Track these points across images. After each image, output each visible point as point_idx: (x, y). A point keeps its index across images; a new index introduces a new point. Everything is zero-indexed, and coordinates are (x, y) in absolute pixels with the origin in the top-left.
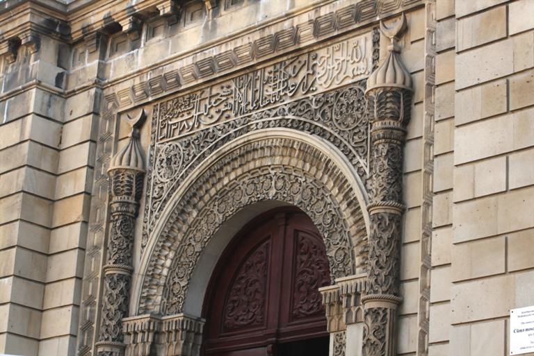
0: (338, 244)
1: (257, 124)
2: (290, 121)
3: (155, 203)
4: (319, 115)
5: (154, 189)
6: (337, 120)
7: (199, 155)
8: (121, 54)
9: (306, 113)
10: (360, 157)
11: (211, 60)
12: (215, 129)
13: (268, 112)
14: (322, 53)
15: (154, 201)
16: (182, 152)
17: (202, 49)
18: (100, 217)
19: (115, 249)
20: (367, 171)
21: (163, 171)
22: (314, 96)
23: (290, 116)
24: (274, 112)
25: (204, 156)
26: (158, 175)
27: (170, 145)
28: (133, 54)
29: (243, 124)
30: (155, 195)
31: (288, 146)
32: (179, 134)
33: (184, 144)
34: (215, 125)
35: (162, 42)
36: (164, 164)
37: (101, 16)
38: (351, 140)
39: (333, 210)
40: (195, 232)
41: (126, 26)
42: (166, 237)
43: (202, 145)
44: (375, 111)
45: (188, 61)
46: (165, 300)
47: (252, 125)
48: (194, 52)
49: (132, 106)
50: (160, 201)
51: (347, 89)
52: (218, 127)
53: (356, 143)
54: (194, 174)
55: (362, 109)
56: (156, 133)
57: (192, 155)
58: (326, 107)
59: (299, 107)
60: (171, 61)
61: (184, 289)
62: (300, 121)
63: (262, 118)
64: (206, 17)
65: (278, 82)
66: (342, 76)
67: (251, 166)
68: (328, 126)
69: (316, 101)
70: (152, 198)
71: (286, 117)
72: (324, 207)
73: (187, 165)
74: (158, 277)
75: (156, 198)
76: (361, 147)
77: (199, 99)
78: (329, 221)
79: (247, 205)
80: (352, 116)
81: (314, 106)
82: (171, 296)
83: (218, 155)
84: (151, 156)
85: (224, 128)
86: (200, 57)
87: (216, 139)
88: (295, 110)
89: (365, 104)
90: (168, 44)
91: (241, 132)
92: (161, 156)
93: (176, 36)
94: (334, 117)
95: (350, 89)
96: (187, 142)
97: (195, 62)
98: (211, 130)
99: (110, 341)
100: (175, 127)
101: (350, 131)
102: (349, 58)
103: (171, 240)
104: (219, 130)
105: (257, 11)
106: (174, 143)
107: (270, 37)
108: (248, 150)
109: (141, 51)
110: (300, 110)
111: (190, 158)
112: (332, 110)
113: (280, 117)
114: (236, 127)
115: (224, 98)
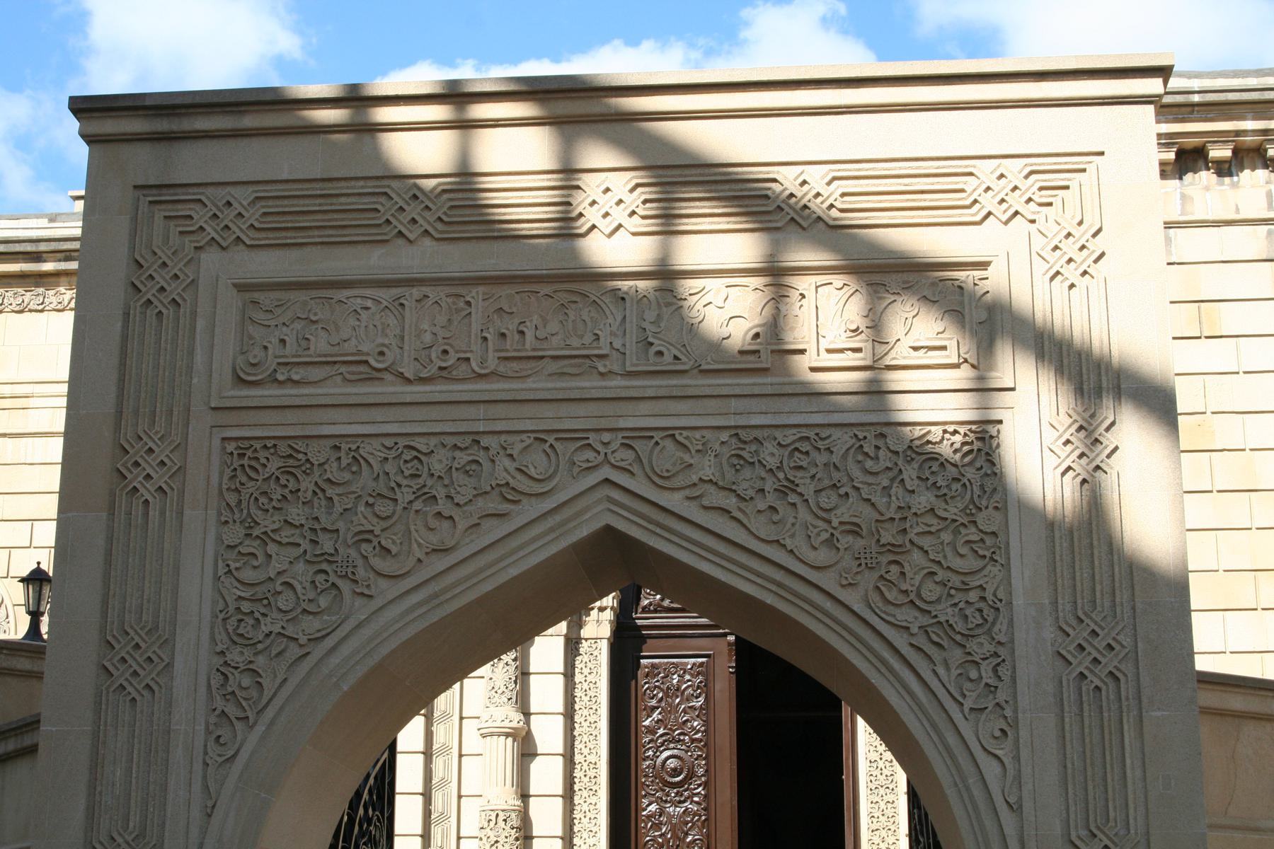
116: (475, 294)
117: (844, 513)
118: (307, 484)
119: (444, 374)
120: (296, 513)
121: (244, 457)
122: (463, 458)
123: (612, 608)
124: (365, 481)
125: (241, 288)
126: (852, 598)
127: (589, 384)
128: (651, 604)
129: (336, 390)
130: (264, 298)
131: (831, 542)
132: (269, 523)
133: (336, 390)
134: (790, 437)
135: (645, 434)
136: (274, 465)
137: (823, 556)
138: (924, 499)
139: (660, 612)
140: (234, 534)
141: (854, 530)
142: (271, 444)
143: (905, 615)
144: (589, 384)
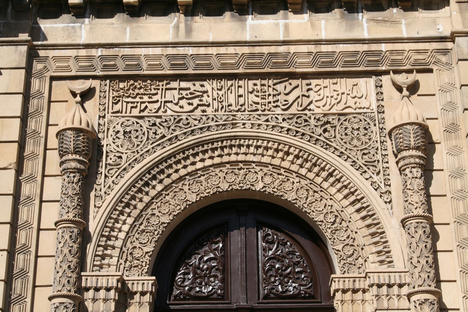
0: (345, 240)
1: (244, 124)
2: (286, 129)
3: (112, 169)
4: (320, 131)
5: (107, 156)
6: (342, 139)
7: (169, 136)
8: (56, 23)
9: (305, 126)
10: (373, 174)
12: (189, 118)
13: (256, 116)
14: (314, 82)
15: (109, 167)
16: (145, 130)
17: (175, 45)
18: (32, 170)
19: (73, 204)
20: (382, 185)
21: (119, 142)
22: (313, 114)
23: (285, 124)
24: (266, 118)
26: (112, 144)
27: (128, 120)
28: (74, 27)
29: (225, 121)
30: (109, 161)
32: (140, 113)
33: (147, 123)
34: (189, 114)
35: (115, 26)
36: (121, 135)
38: (360, 158)
39: (336, 212)
40: (159, 204)
43: (172, 127)
44: (412, 140)
46: (122, 261)
47: (236, 124)
49: (73, 73)
50: (119, 169)
51: (351, 116)
52: (194, 117)
53: (366, 162)
54: (160, 153)
55: (370, 136)
56: (107, 105)
57: (160, 135)
58: (328, 126)
59: (295, 120)
61: (149, 254)
62: (297, 132)
63: (250, 120)
64: (176, 19)
65: (267, 93)
66: (341, 106)
67: (233, 158)
68: (332, 142)
69: (315, 118)
70: (106, 164)
71: (280, 125)
72: (325, 207)
73: (153, 143)
74: (114, 239)
75: (110, 165)
76: (373, 166)
77: (164, 87)
78: (332, 220)
79: (227, 190)
80: (359, 139)
81: (312, 122)
82: (130, 258)
83: (196, 141)
84: (99, 124)
85: (201, 118)
87: (191, 127)
88: (291, 121)
89: (372, 132)
90: (125, 29)
92: (114, 127)
93: (135, 25)
94: (338, 136)
95: (355, 117)
96: (152, 122)
97: (165, 54)
98: (184, 118)
99: (72, 293)
100: (133, 105)
101: (358, 150)
102: (350, 92)
103: (132, 207)
104: (196, 120)
105: (244, 28)
106: (135, 120)
107: (261, 55)
110: (296, 123)
111: (158, 137)
112: (335, 130)
113: (274, 124)
114: (216, 121)
115: (198, 94)
123: (151, 293)
128: (181, 293)
139: (188, 300)
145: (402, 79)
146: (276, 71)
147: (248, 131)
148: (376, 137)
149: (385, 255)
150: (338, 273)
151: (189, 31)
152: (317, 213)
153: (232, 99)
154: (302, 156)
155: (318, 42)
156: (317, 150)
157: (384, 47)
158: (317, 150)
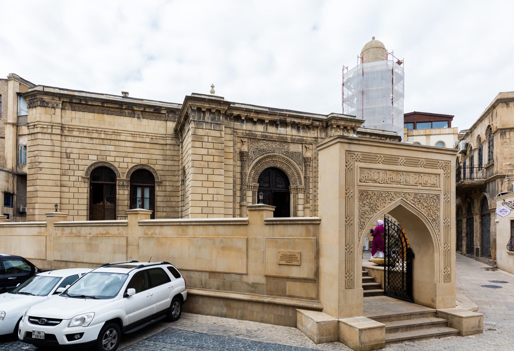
11: (266, 135)
17: (264, 132)
25: (263, 154)
31: (284, 159)
37: (238, 113)
41: (243, 118)
42: (253, 168)
45: (260, 133)
48: (262, 132)
54: (260, 157)
60: (255, 131)
86: (263, 134)
91: (273, 153)
108: (274, 156)
109: (245, 125)
116: (387, 172)
117: (425, 204)
118: (369, 197)
119: (384, 183)
120: (368, 201)
121: (361, 193)
122: (386, 195)
124: (375, 197)
125: (360, 168)
126: (425, 215)
127: (399, 186)
129: (371, 184)
130: (363, 170)
131: (424, 208)
132: (365, 202)
133: (371, 184)
134: (420, 194)
135: (405, 193)
136: (365, 194)
137: (423, 210)
138: (432, 204)
140: (361, 203)
141: (426, 207)
142: (365, 191)
143: (430, 217)
144: (399, 186)
145: (307, 145)
146: (283, 140)
147: (278, 154)
148: (301, 158)
149: (301, 182)
150: (291, 185)
151: (267, 129)
152: (289, 172)
153: (274, 146)
154: (287, 160)
155: (292, 136)
156: (290, 159)
157: (305, 138)
158: (290, 159)
